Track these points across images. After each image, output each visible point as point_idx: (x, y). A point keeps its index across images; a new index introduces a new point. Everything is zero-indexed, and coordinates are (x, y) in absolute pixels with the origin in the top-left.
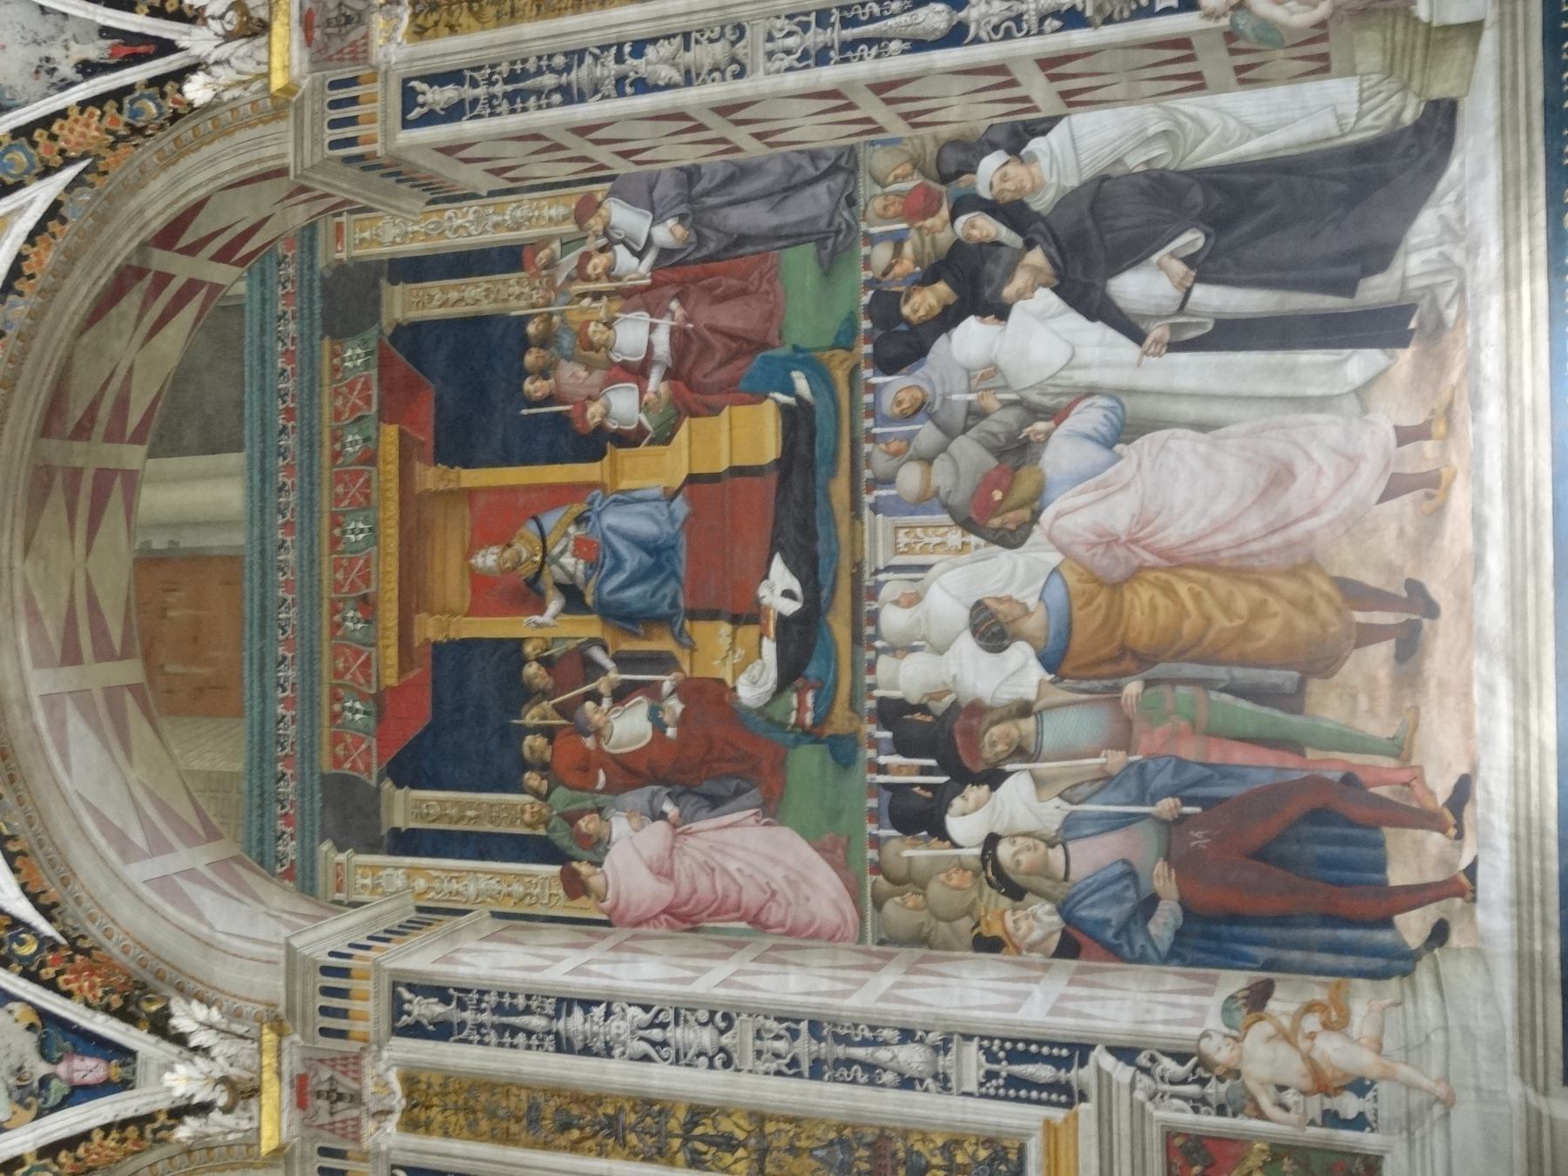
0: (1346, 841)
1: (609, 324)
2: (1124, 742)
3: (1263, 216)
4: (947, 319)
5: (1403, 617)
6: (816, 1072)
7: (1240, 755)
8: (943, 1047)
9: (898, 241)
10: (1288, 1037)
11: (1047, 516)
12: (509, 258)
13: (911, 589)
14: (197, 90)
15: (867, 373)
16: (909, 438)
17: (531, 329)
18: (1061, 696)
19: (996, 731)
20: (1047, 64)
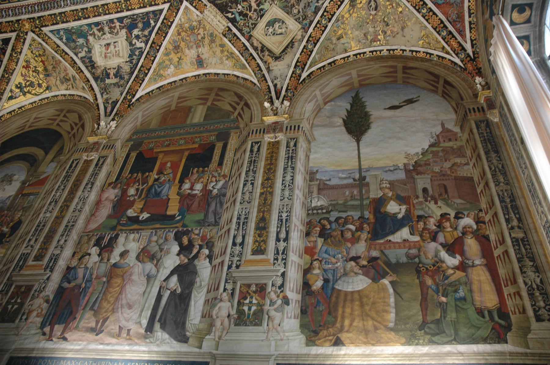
1: (202, 182)
4: (181, 245)
5: (98, 329)
6: (67, 226)
7: (87, 298)
8: (62, 247)
9: (198, 235)
11: (139, 264)
12: (220, 164)
14: (267, 105)
15: (176, 230)
16: (162, 238)
17: (206, 169)
18: (109, 266)
19: (107, 255)
20: (223, 262)
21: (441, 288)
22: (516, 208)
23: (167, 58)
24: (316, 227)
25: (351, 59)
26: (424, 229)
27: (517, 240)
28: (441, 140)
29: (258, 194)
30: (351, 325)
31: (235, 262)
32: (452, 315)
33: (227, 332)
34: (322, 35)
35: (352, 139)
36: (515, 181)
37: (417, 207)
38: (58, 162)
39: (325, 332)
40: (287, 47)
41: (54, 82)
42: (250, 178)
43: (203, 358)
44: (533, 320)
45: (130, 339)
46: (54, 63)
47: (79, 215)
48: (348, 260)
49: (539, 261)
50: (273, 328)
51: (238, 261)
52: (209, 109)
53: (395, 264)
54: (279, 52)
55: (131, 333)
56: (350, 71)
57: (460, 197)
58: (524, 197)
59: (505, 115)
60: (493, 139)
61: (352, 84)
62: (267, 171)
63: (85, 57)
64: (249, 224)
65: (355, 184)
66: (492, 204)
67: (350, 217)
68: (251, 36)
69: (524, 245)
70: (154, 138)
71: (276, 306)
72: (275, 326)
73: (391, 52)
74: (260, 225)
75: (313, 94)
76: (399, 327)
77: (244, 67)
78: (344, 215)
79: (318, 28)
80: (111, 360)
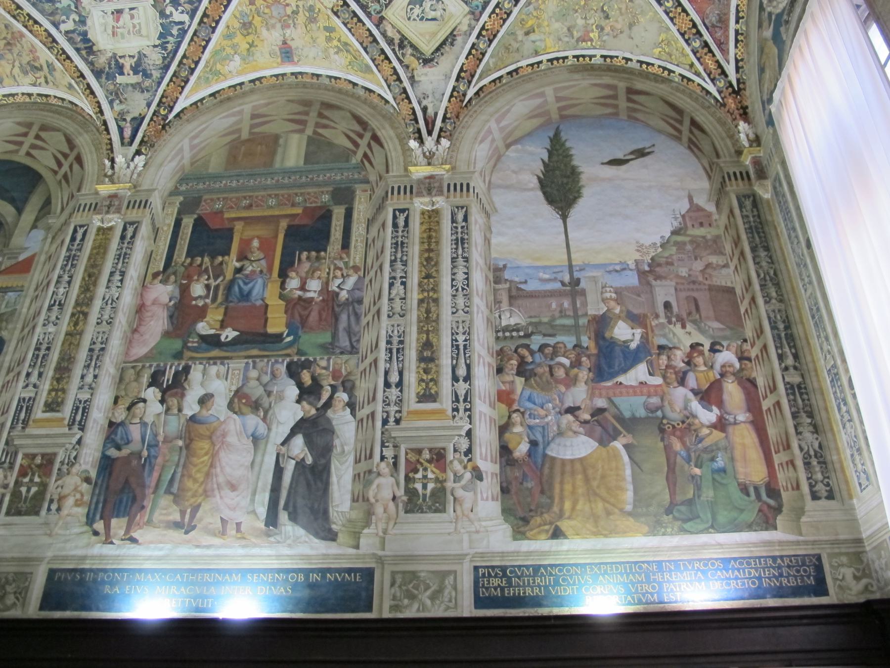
0: (126, 507)
1: (319, 278)
2: (166, 440)
3: (312, 482)
4: (300, 385)
5: (186, 524)
6: (91, 350)
7: (156, 475)
8: (91, 388)
9: (325, 368)
10: (75, 489)
11: (235, 416)
12: (346, 245)
13: (221, 375)
14: (413, 144)
15: (288, 359)
16: (266, 373)
17: (323, 253)
18: (183, 421)
19: (175, 401)
20: (373, 414)
21: (693, 455)
22: (791, 338)
23: (229, 43)
25: (542, 67)
26: (668, 367)
27: (792, 387)
28: (689, 224)
29: (415, 302)
30: (573, 509)
31: (392, 414)
32: (708, 493)
33: (395, 523)
34: (501, 26)
35: (554, 212)
36: (791, 296)
38: (48, 228)
39: (538, 520)
40: (444, 43)
41: (8, 71)
42: (399, 274)
43: (363, 563)
44: (808, 497)
45: (244, 538)
46: (9, 36)
47: (110, 331)
48: (563, 412)
49: (818, 418)
50: (463, 515)
51: (397, 412)
52: (311, 141)
53: (629, 419)
54: (431, 51)
55: (243, 528)
56: (542, 90)
57: (717, 319)
58: (802, 323)
59: (784, 196)
60: (762, 228)
61: (547, 113)
62: (425, 263)
63: (73, 31)
64: (407, 352)
65: (565, 291)
66: (760, 332)
67: (561, 345)
68: (382, 19)
69: (801, 394)
70: (220, 191)
71: (463, 482)
72: (466, 513)
73: (608, 60)
74: (425, 354)
75: (486, 128)
76: (640, 510)
77: (368, 69)
78: (551, 341)
79: (497, 15)
80: (219, 571)
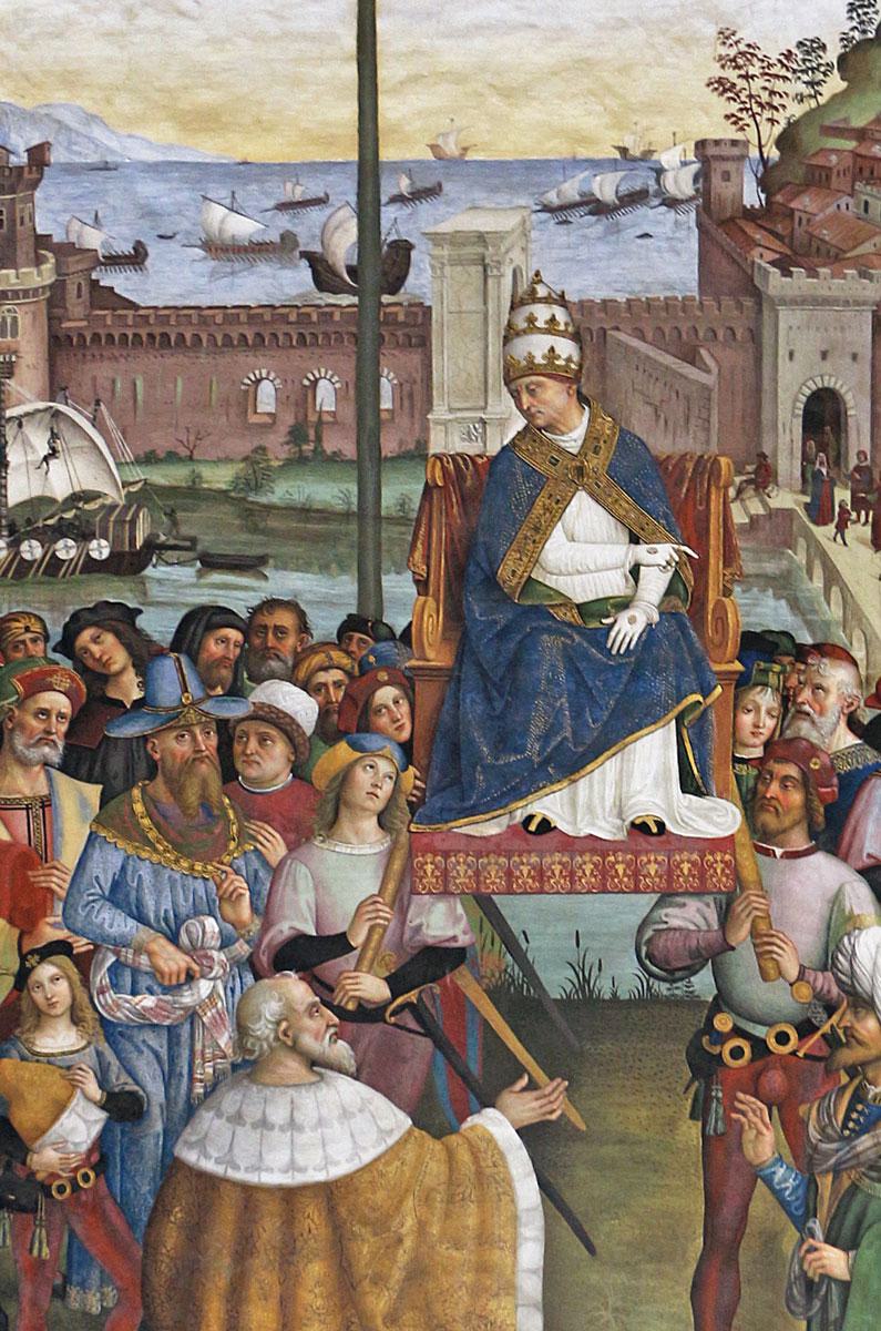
21: (826, 1183)
24: (38, 685)
37: (749, 565)
53: (565, 1004)
65: (326, 314)
67: (286, 619)
78: (240, 594)
